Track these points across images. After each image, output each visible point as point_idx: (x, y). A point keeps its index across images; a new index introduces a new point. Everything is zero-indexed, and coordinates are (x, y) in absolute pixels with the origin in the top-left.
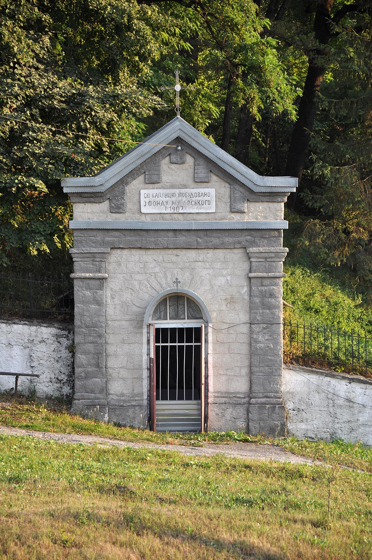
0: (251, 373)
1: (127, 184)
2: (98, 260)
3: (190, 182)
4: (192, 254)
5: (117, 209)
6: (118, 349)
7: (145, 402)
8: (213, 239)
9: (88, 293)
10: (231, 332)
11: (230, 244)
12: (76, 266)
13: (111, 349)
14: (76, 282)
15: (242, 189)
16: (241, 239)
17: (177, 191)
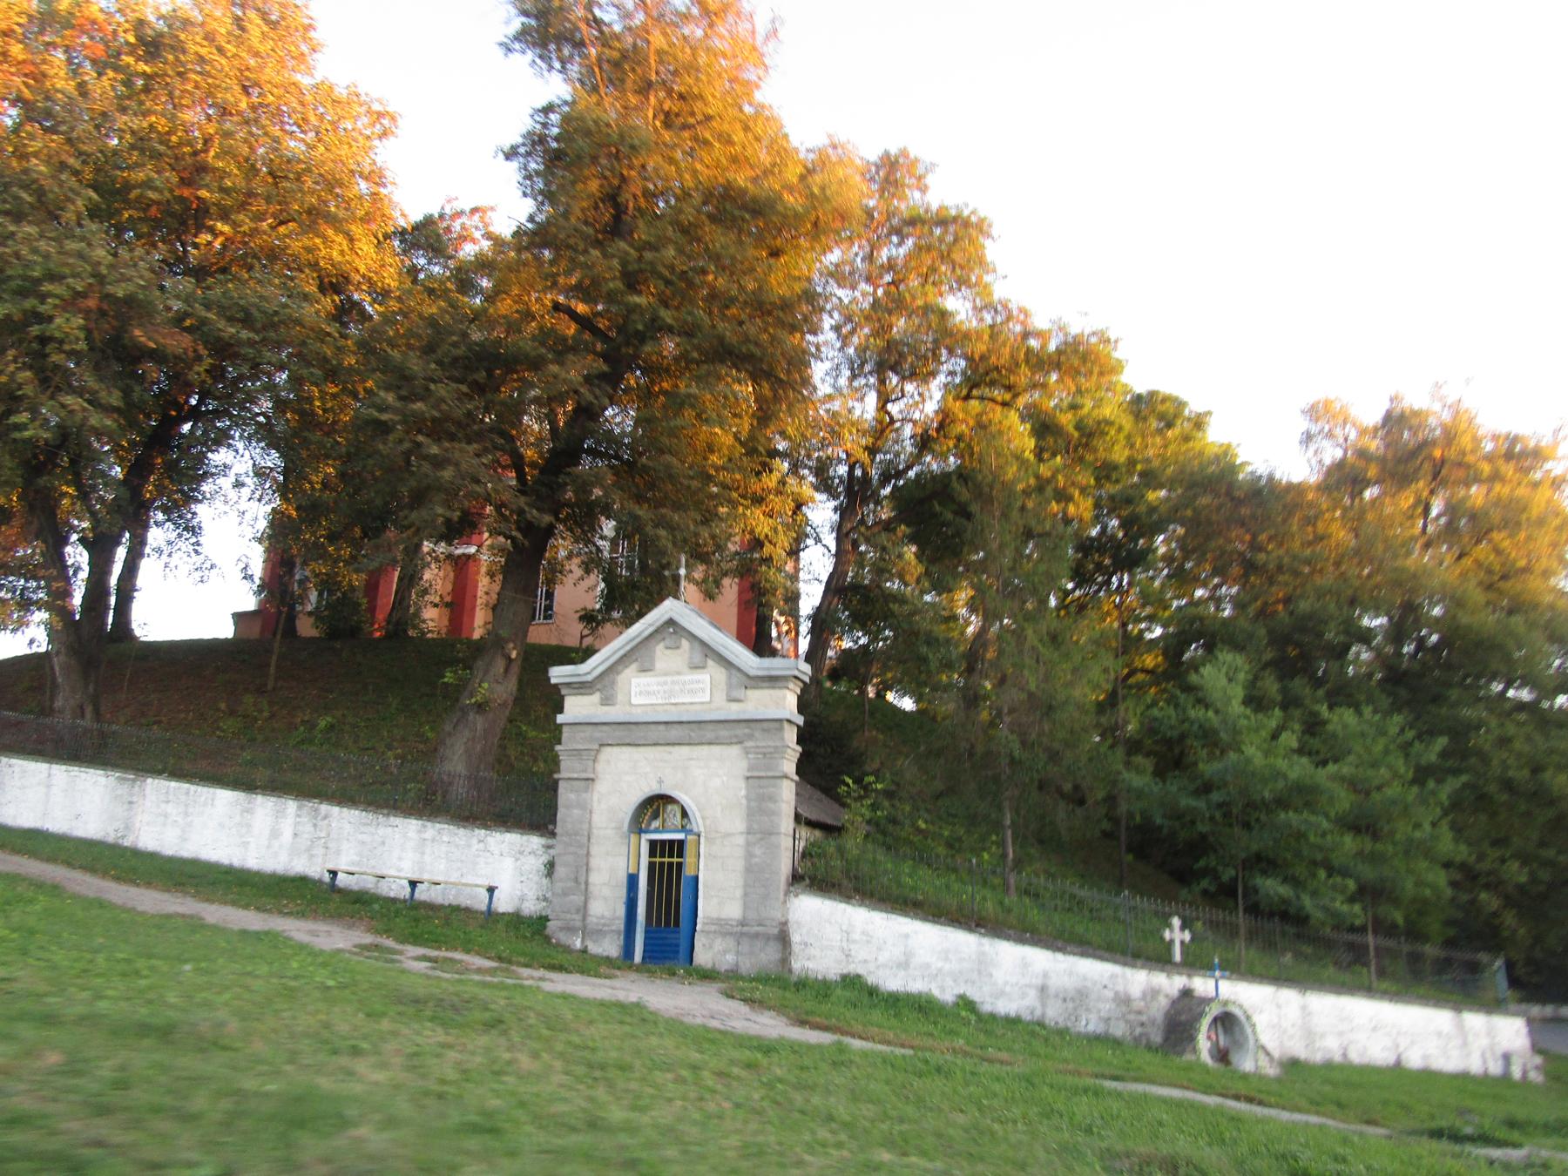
0: (746, 894)
1: (618, 673)
4: (685, 750)
5: (607, 701)
9: (572, 796)
12: (563, 765)
13: (594, 862)
14: (561, 785)
17: (669, 679)
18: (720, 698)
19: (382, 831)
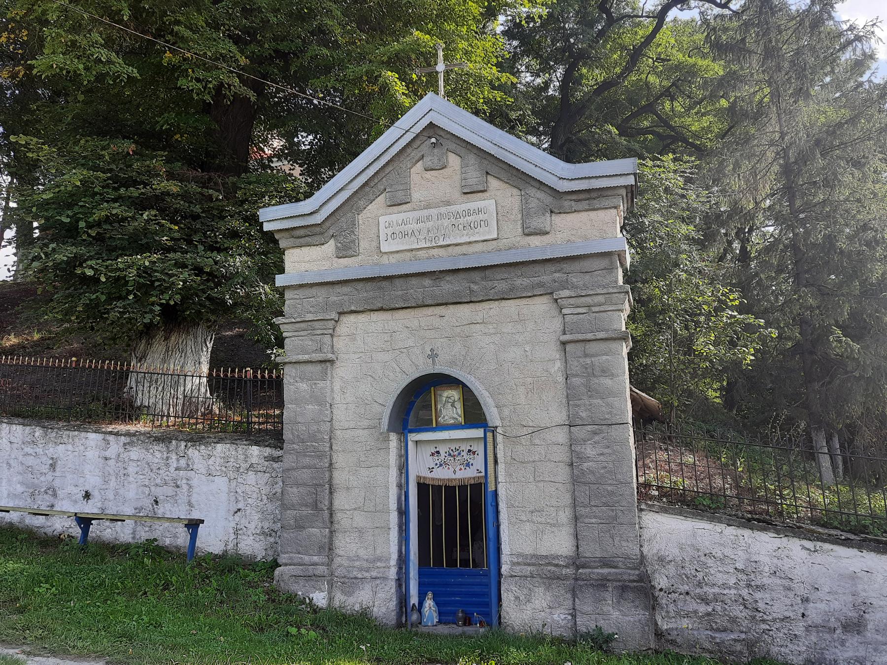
0: (576, 518)
1: (360, 211)
2: (319, 332)
3: (457, 194)
4: (464, 312)
6: (351, 478)
7: (393, 573)
8: (496, 283)
9: (304, 386)
10: (537, 441)
11: (525, 288)
13: (339, 477)
15: (540, 195)
16: (545, 278)
17: (434, 212)
18: (513, 233)
19: (51, 450)
